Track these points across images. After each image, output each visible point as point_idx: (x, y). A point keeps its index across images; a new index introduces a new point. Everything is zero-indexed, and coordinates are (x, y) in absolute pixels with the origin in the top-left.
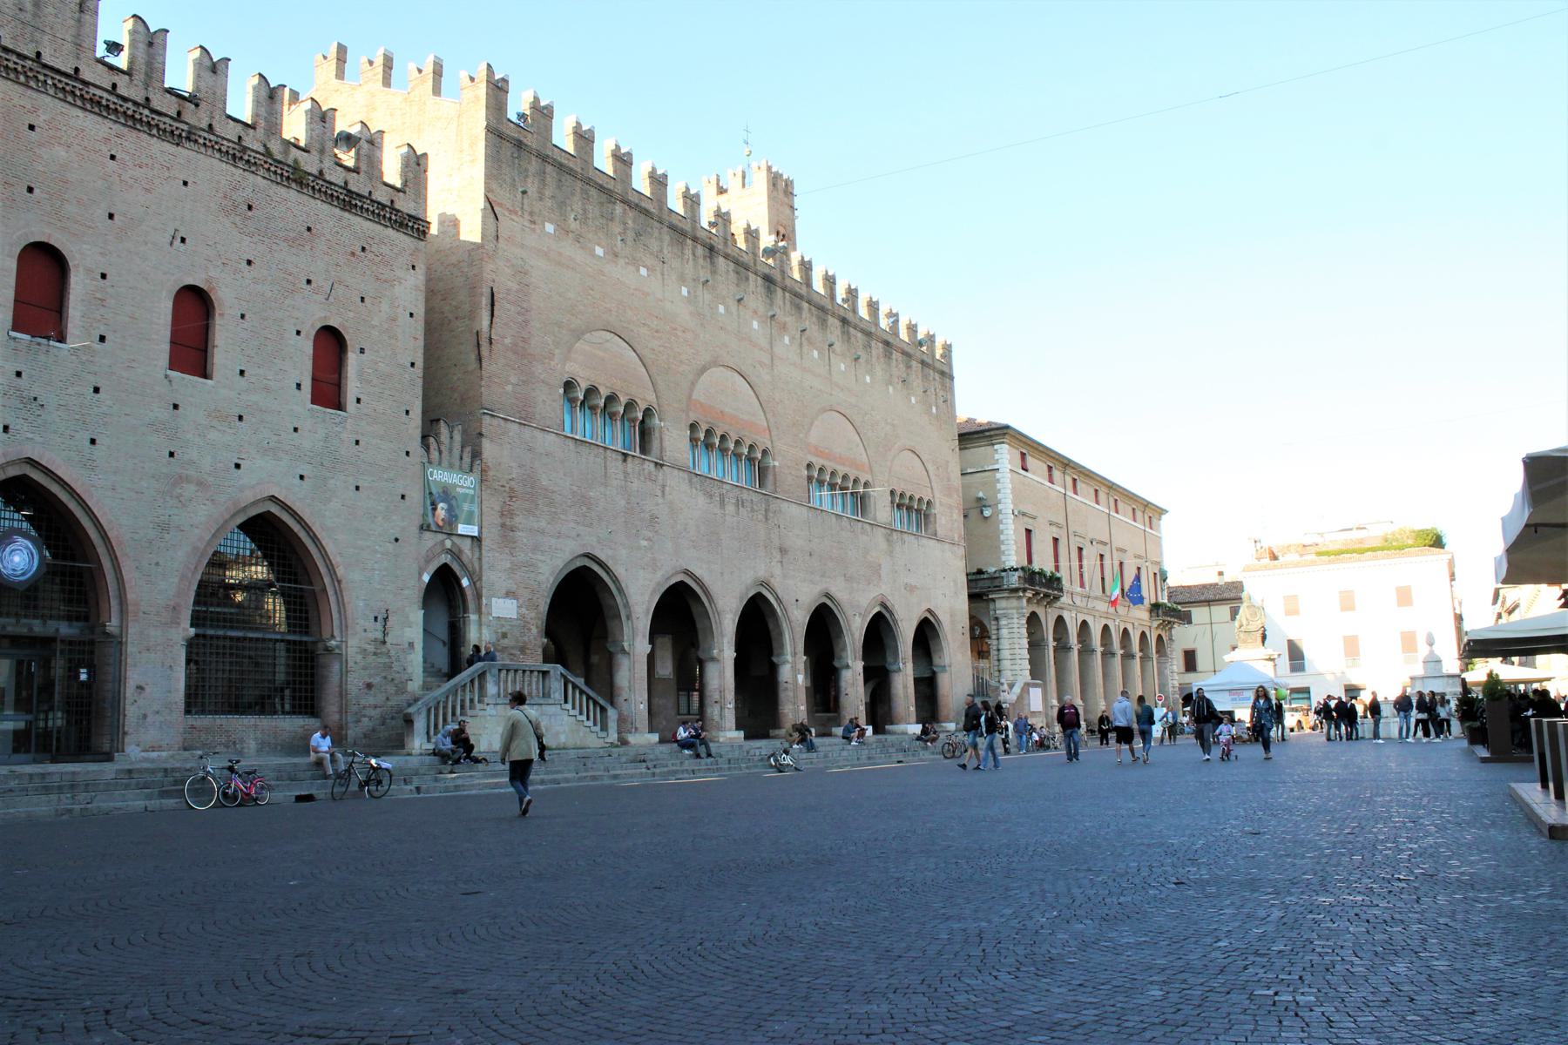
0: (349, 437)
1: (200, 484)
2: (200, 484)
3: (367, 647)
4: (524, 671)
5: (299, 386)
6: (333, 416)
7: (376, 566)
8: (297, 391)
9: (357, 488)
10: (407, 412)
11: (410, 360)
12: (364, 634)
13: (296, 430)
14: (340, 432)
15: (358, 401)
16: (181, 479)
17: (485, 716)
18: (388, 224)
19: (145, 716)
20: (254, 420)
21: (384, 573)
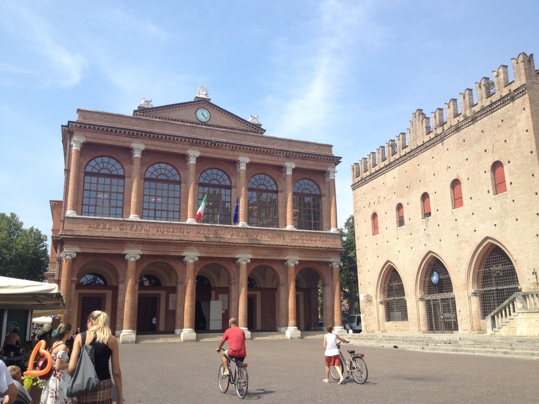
0: (509, 201)
1: (466, 242)
2: (466, 242)
3: (531, 287)
4: (532, 295)
5: (488, 192)
6: (502, 196)
7: (530, 250)
8: (488, 194)
9: (517, 220)
10: (533, 175)
11: (530, 151)
12: (528, 281)
13: (490, 208)
14: (506, 201)
15: (511, 183)
16: (461, 242)
17: (517, 319)
18: (509, 102)
19: (462, 320)
20: (477, 212)
21: (534, 252)
